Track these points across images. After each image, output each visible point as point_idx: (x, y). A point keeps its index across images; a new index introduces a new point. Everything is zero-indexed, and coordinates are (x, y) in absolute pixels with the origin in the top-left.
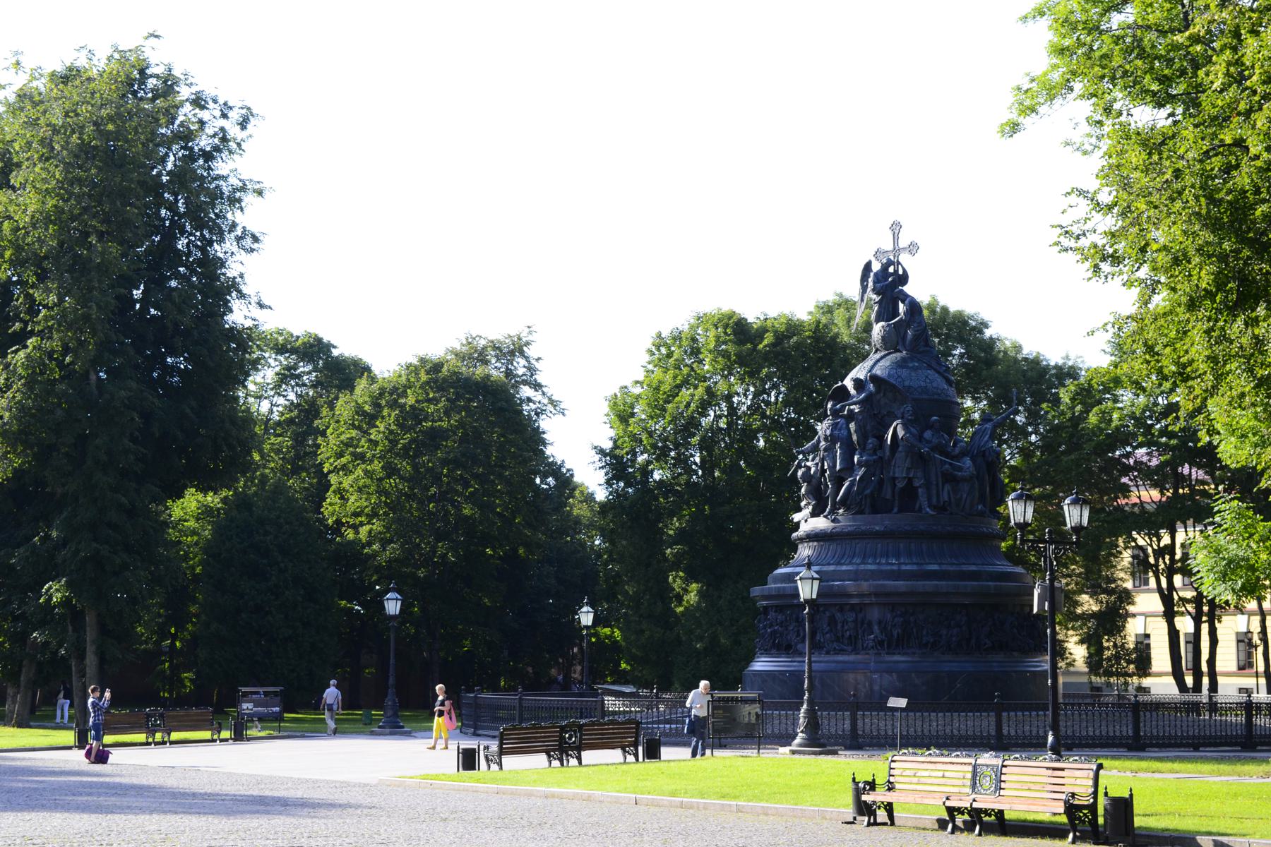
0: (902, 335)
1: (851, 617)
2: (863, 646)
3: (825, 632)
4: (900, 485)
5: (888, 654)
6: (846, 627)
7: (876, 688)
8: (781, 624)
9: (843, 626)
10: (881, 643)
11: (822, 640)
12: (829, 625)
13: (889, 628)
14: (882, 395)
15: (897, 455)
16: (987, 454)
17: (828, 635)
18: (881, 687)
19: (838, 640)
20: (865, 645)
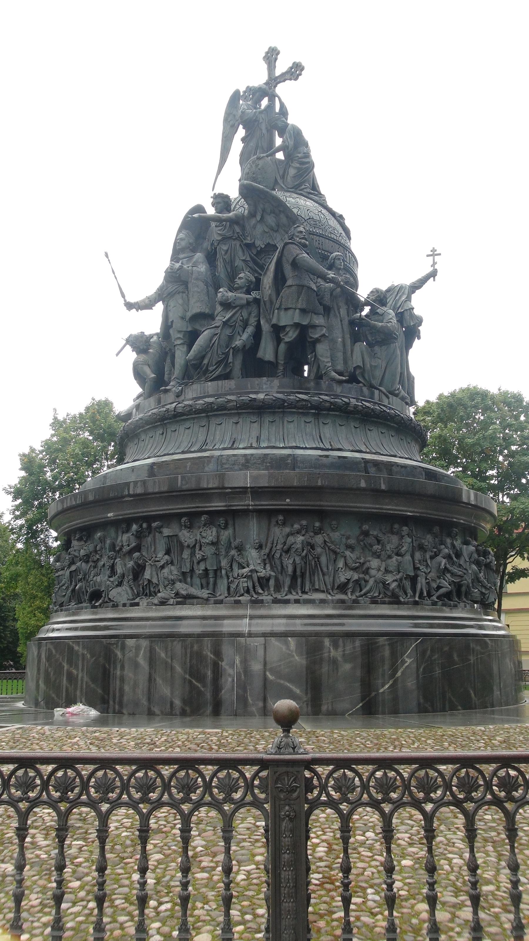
0: (281, 173)
1: (210, 534)
2: (229, 588)
3: (160, 564)
4: (291, 336)
5: (276, 601)
6: (199, 555)
7: (256, 667)
8: (86, 559)
9: (193, 554)
10: (264, 582)
11: (155, 580)
12: (168, 552)
13: (277, 555)
14: (258, 218)
15: (285, 292)
16: (407, 315)
17: (166, 571)
18: (265, 664)
19: (184, 576)
20: (233, 586)
